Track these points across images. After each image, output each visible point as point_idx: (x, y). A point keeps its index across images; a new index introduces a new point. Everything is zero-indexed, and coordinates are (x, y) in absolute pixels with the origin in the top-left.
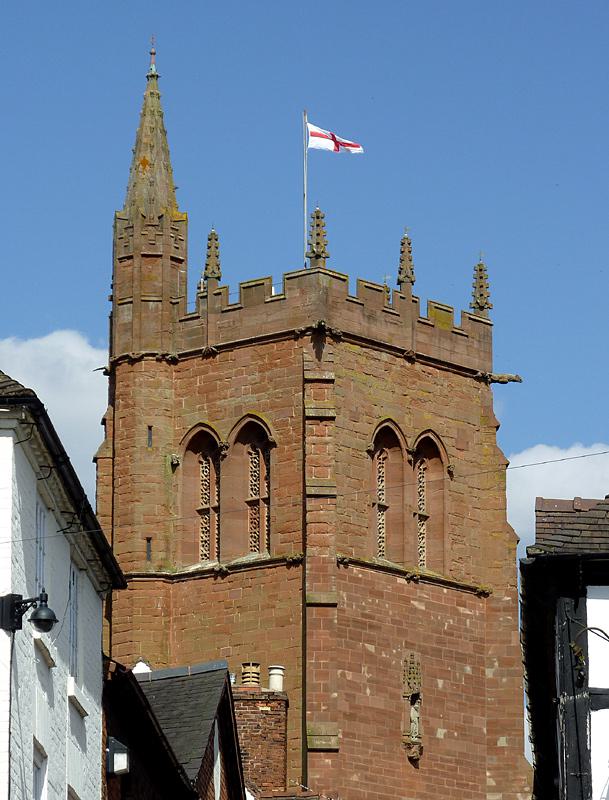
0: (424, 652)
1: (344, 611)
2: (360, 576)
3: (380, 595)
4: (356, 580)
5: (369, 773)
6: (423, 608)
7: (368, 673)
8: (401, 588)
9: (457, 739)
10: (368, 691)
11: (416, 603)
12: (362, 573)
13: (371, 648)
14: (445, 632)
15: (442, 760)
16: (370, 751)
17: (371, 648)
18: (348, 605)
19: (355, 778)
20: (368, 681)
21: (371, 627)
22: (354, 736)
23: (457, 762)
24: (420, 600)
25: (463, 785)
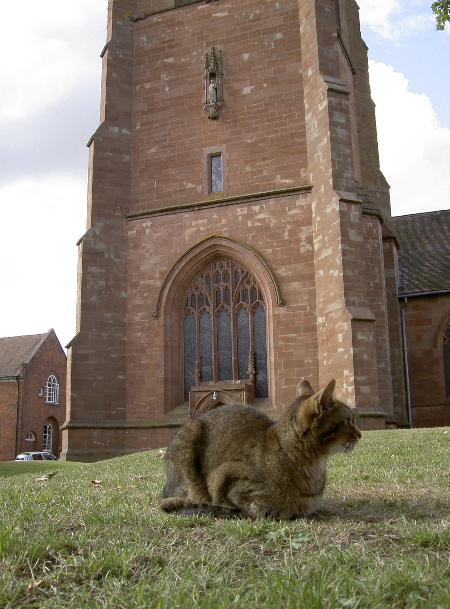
0: (223, 42)
1: (144, 47)
2: (160, 20)
3: (181, 23)
4: (157, 23)
5: (166, 144)
6: (227, 14)
7: (167, 77)
8: (203, 10)
9: (267, 87)
10: (167, 89)
11: (218, 15)
12: (162, 18)
13: (171, 60)
14: (251, 21)
15: (248, 108)
16: (168, 128)
17: (171, 60)
18: (147, 43)
19: (153, 150)
20: (167, 82)
21: (170, 47)
22: (152, 123)
23: (267, 104)
24: (222, 10)
25: (274, 119)
